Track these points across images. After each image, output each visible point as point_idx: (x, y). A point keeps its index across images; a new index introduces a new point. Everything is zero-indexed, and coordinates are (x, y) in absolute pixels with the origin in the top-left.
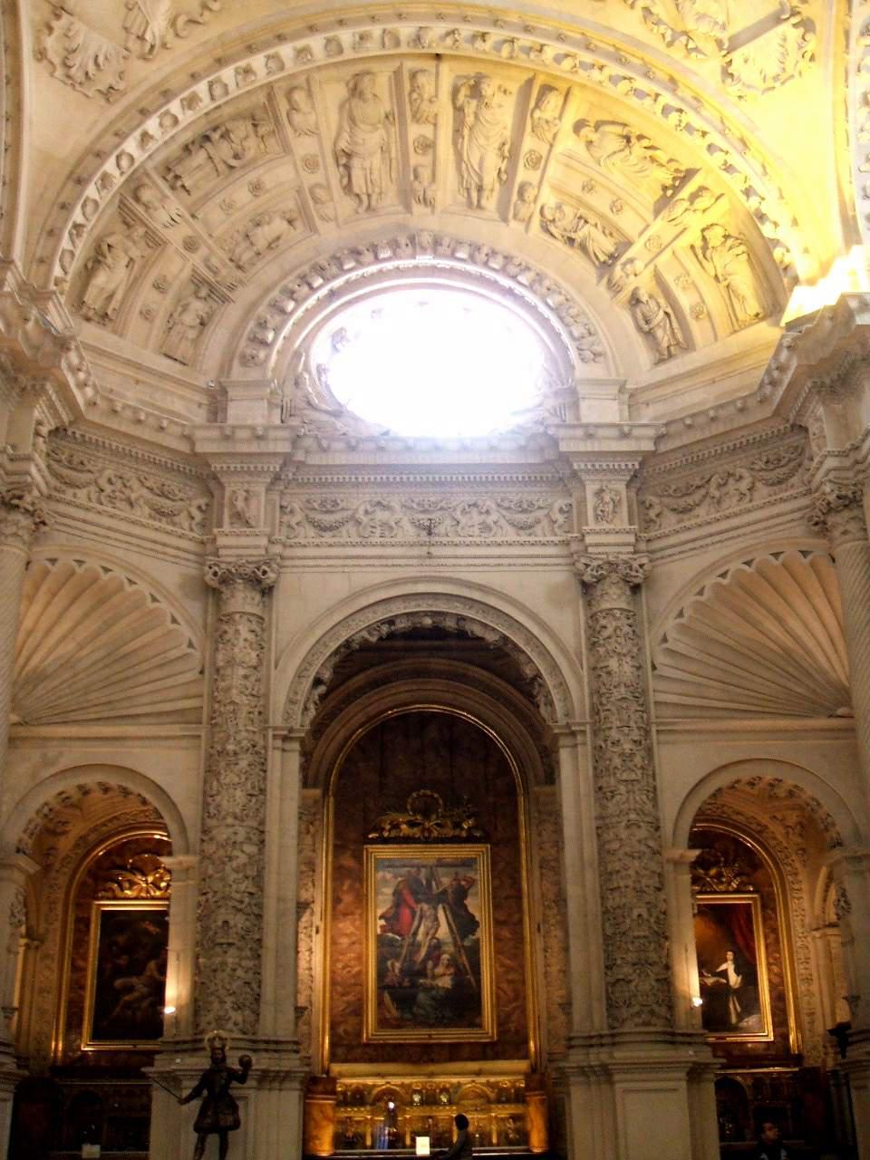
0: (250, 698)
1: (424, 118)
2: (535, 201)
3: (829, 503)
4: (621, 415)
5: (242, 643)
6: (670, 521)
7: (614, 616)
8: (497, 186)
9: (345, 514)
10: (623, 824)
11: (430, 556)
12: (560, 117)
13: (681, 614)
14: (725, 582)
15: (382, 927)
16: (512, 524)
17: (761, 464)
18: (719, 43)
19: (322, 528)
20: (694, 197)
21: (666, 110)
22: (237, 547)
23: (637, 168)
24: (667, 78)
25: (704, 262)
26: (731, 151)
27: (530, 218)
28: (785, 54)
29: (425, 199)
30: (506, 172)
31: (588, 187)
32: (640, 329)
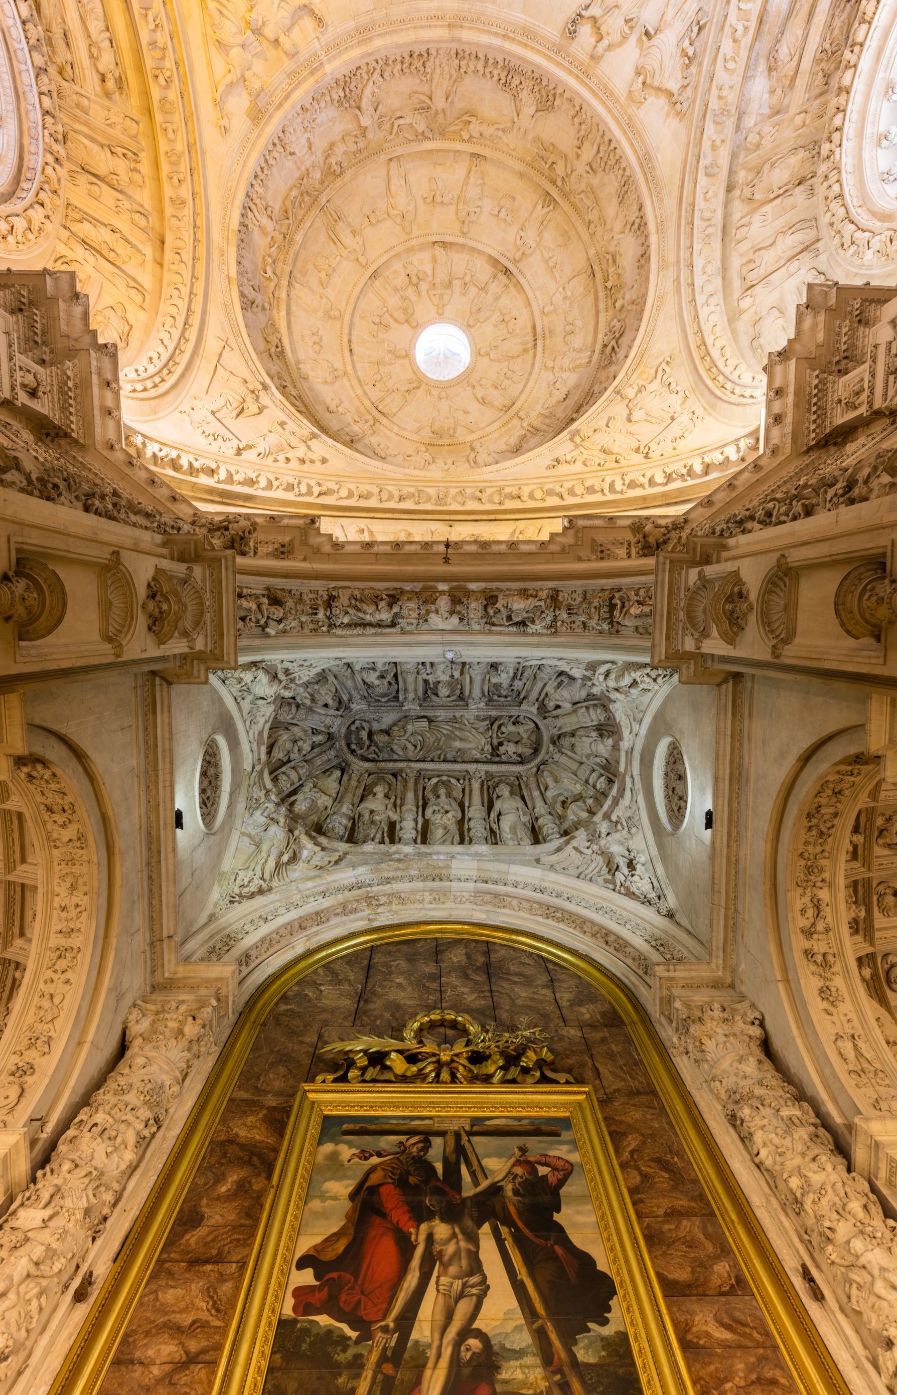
15: (298, 1292)
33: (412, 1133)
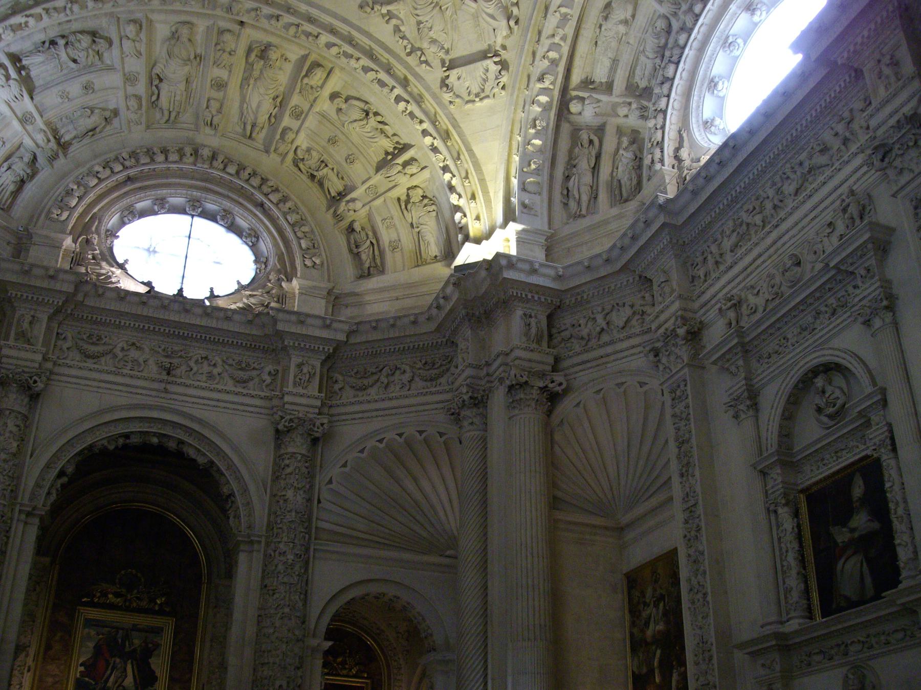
0: (6, 477)
1: (223, 65)
2: (292, 142)
3: (464, 401)
4: (326, 309)
5: (7, 435)
6: (348, 394)
7: (296, 458)
8: (266, 125)
9: (106, 348)
10: (279, 615)
11: (166, 391)
12: (322, 87)
13: (345, 465)
14: (381, 446)
15: (80, 672)
16: (232, 377)
17: (419, 365)
18: (443, 62)
19: (87, 356)
20: (406, 164)
21: (398, 99)
22: (18, 359)
23: (370, 135)
24: (402, 77)
25: (405, 212)
26: (437, 137)
27: (287, 153)
28: (485, 80)
29: (211, 124)
30: (275, 117)
31: (333, 141)
32: (351, 251)
33: (113, 627)
